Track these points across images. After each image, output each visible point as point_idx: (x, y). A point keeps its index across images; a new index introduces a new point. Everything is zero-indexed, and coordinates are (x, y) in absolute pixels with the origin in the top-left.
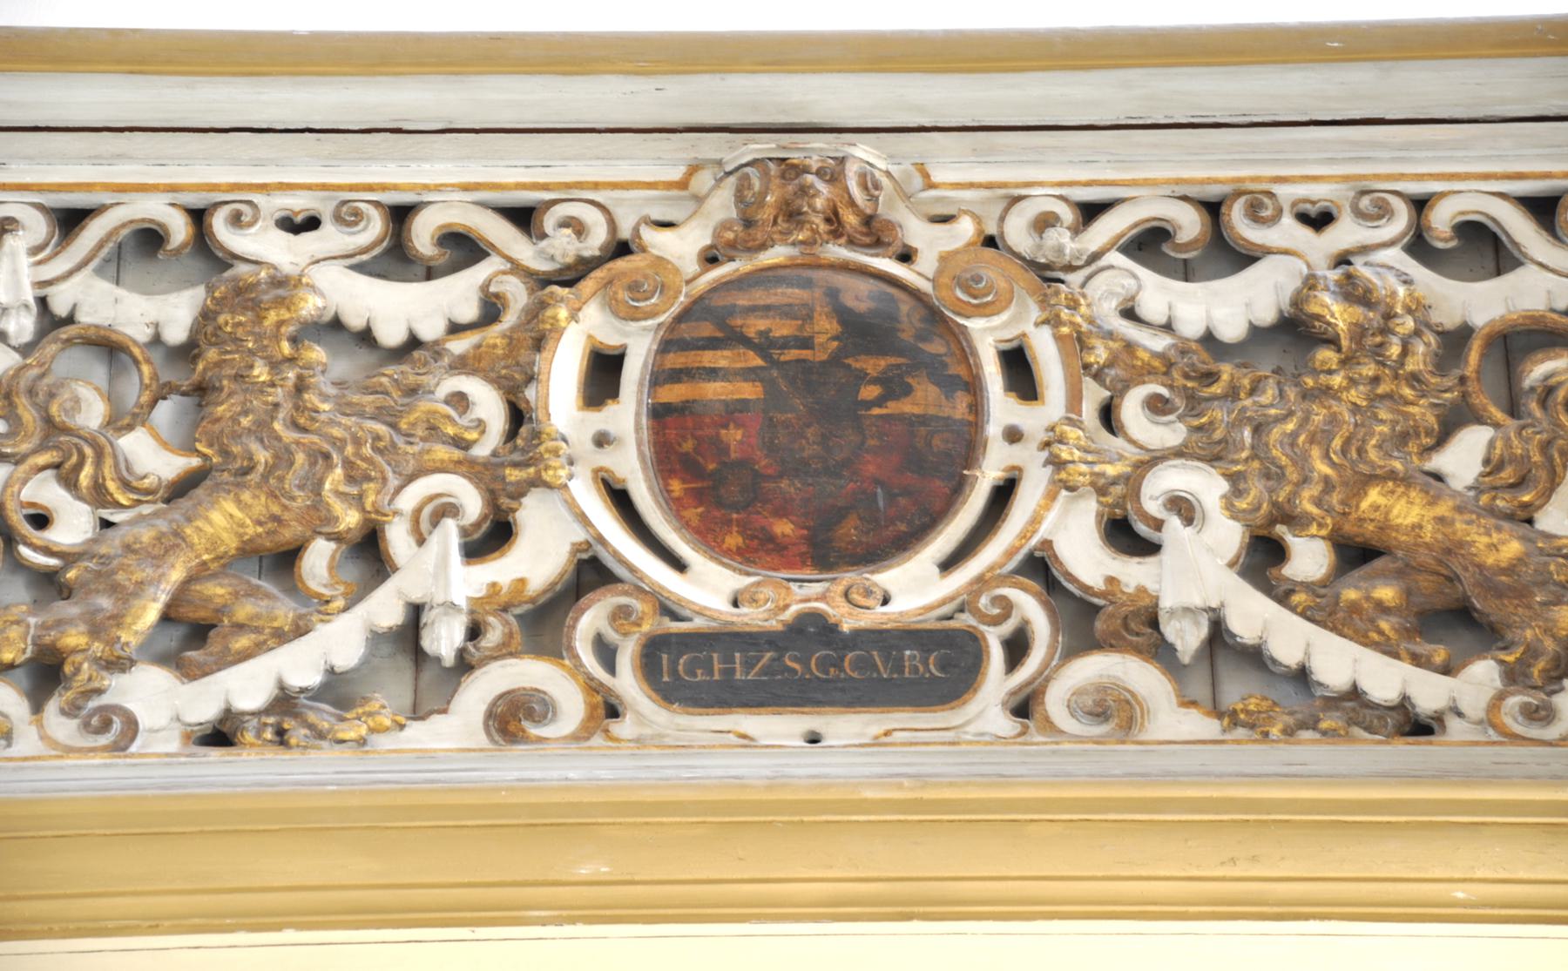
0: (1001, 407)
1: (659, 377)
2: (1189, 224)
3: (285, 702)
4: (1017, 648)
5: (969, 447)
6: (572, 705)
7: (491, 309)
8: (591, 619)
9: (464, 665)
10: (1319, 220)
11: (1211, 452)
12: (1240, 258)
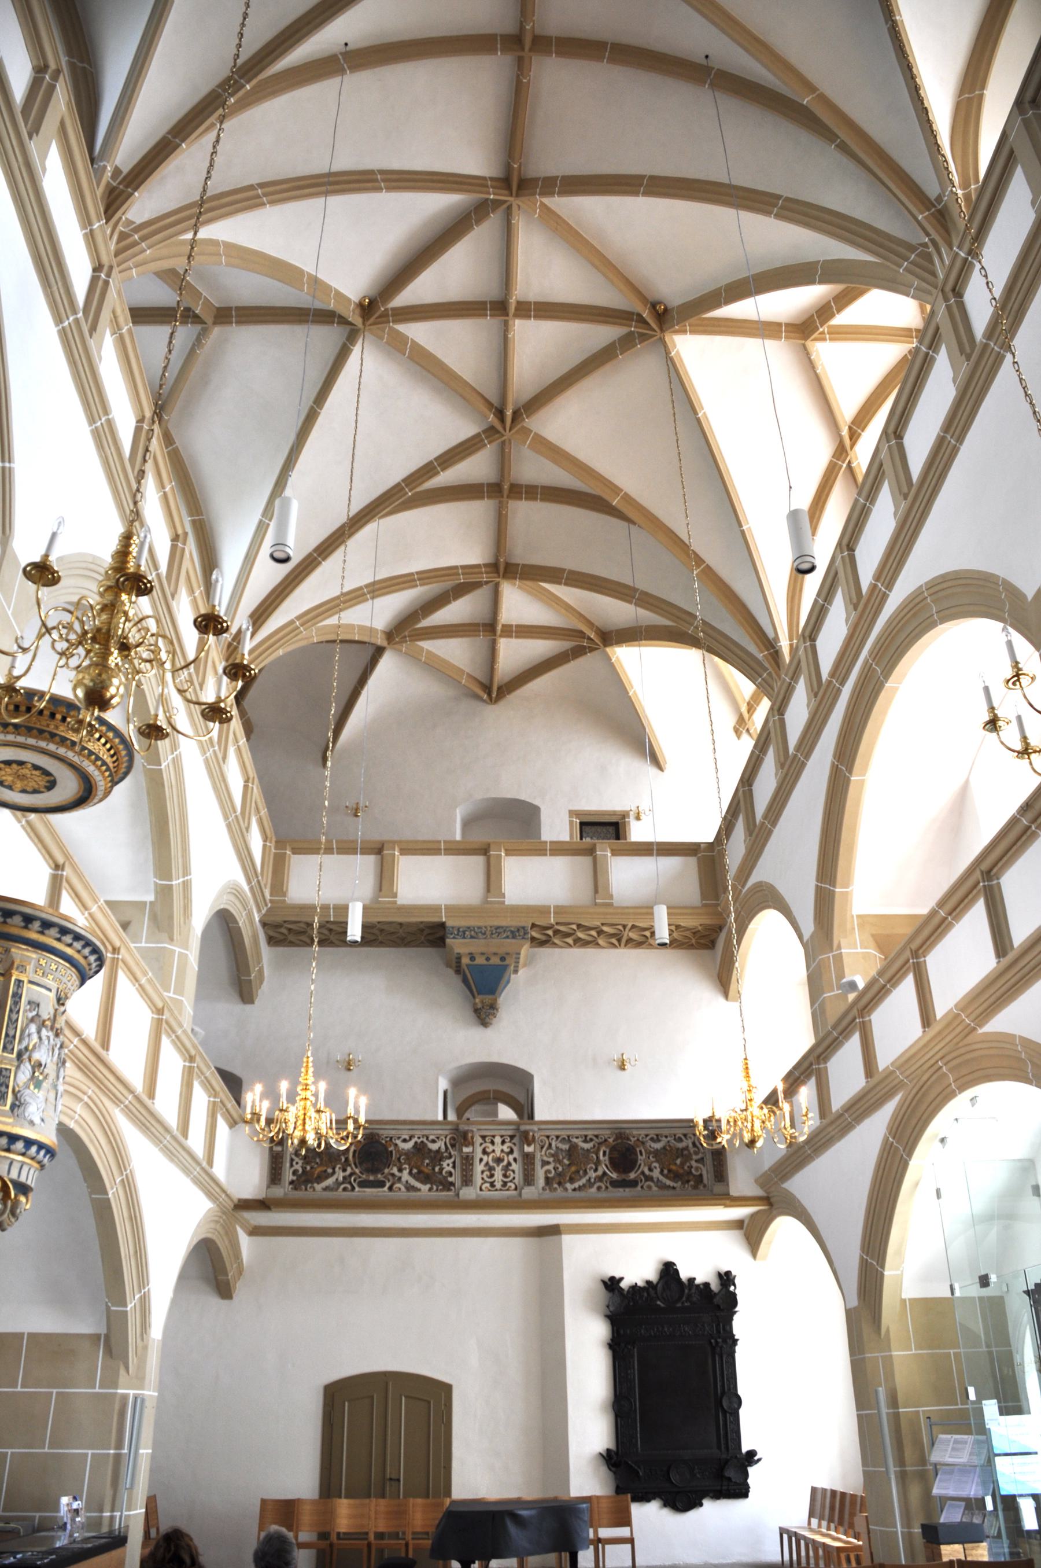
0: (639, 1157)
1: (610, 1154)
2: (655, 1137)
3: (580, 1187)
4: (641, 1181)
5: (636, 1161)
6: (604, 1187)
7: (594, 1146)
8: (605, 1179)
9: (595, 1183)
10: (666, 1137)
11: (657, 1161)
12: (659, 1141)
